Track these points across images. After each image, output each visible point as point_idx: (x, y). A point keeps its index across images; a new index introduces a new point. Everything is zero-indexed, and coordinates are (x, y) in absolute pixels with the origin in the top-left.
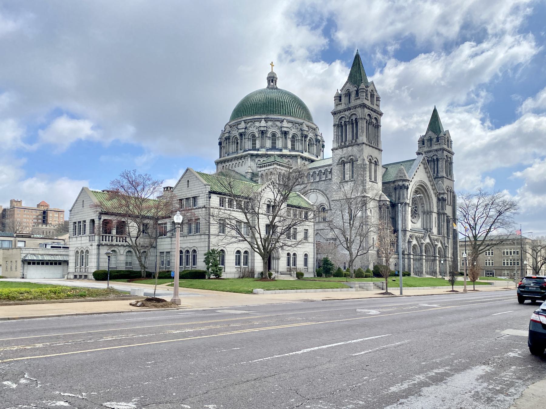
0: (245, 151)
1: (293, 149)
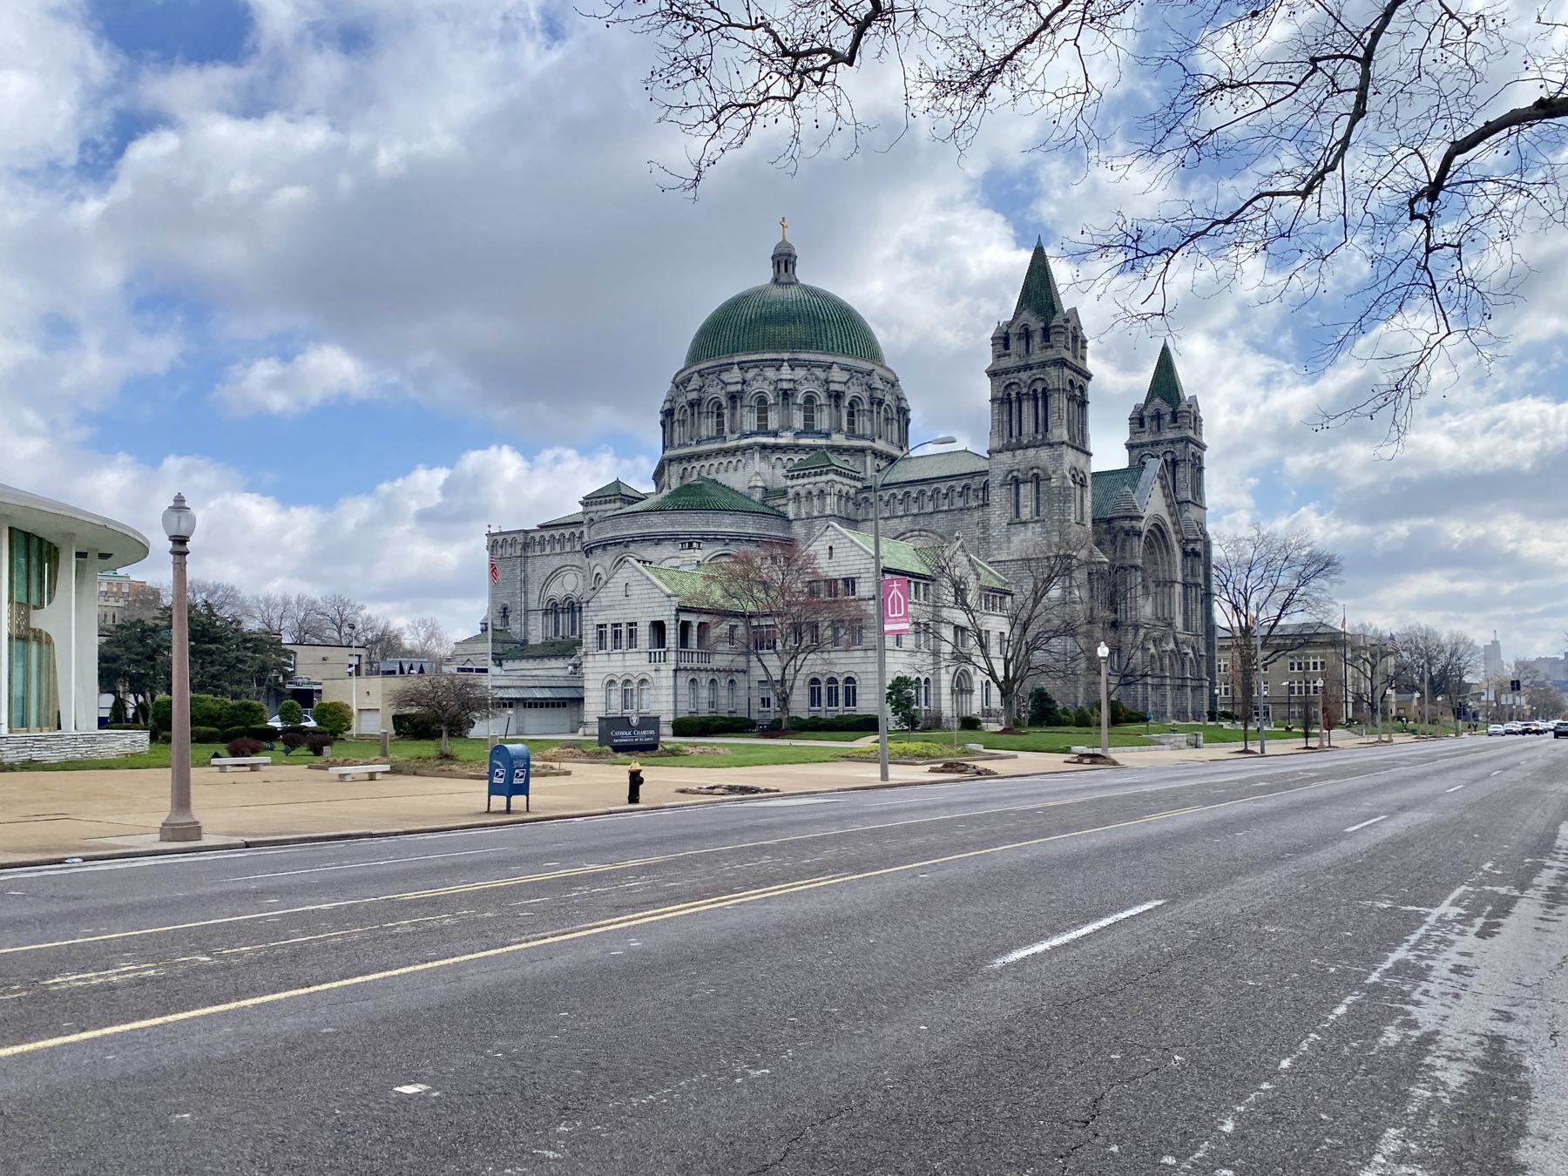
1: (851, 434)
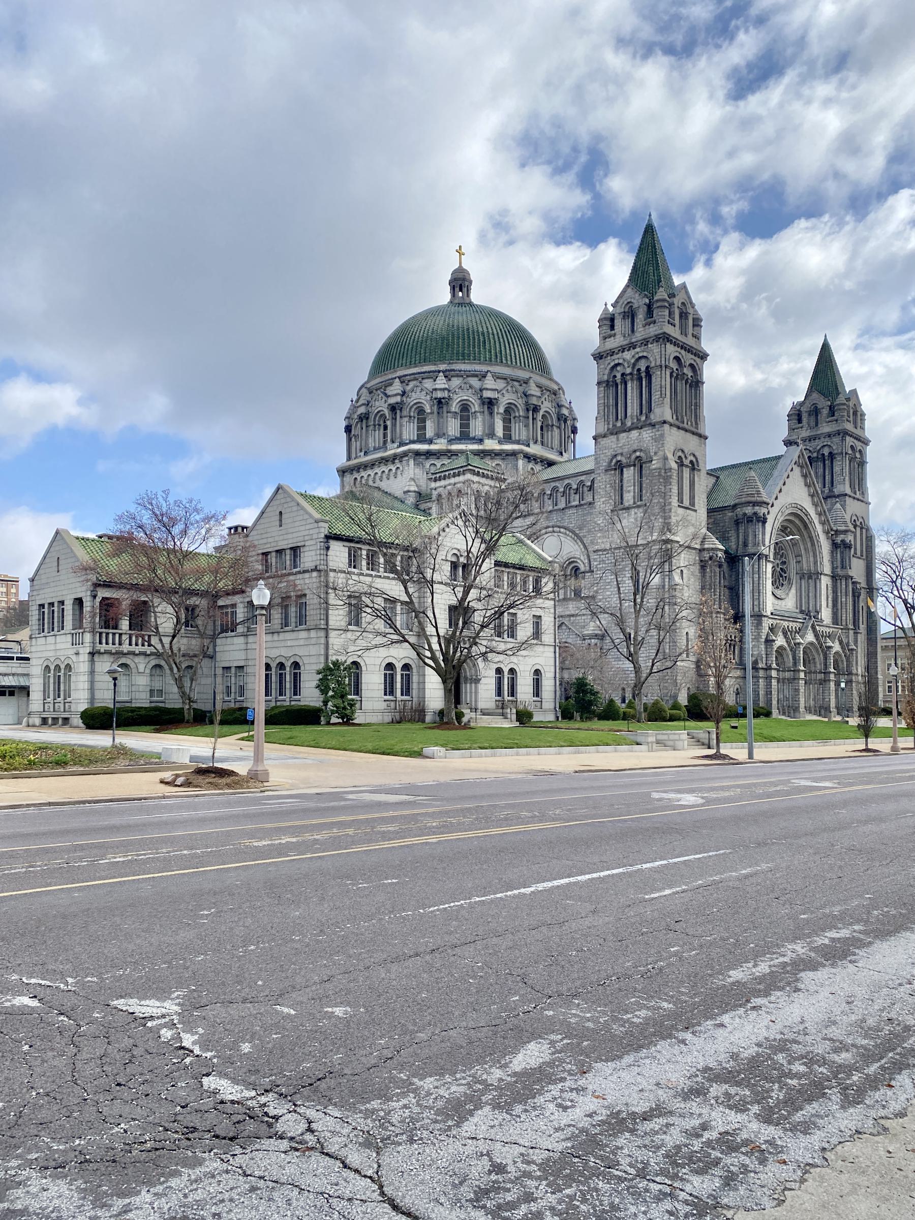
0: (402, 444)
1: (508, 438)
